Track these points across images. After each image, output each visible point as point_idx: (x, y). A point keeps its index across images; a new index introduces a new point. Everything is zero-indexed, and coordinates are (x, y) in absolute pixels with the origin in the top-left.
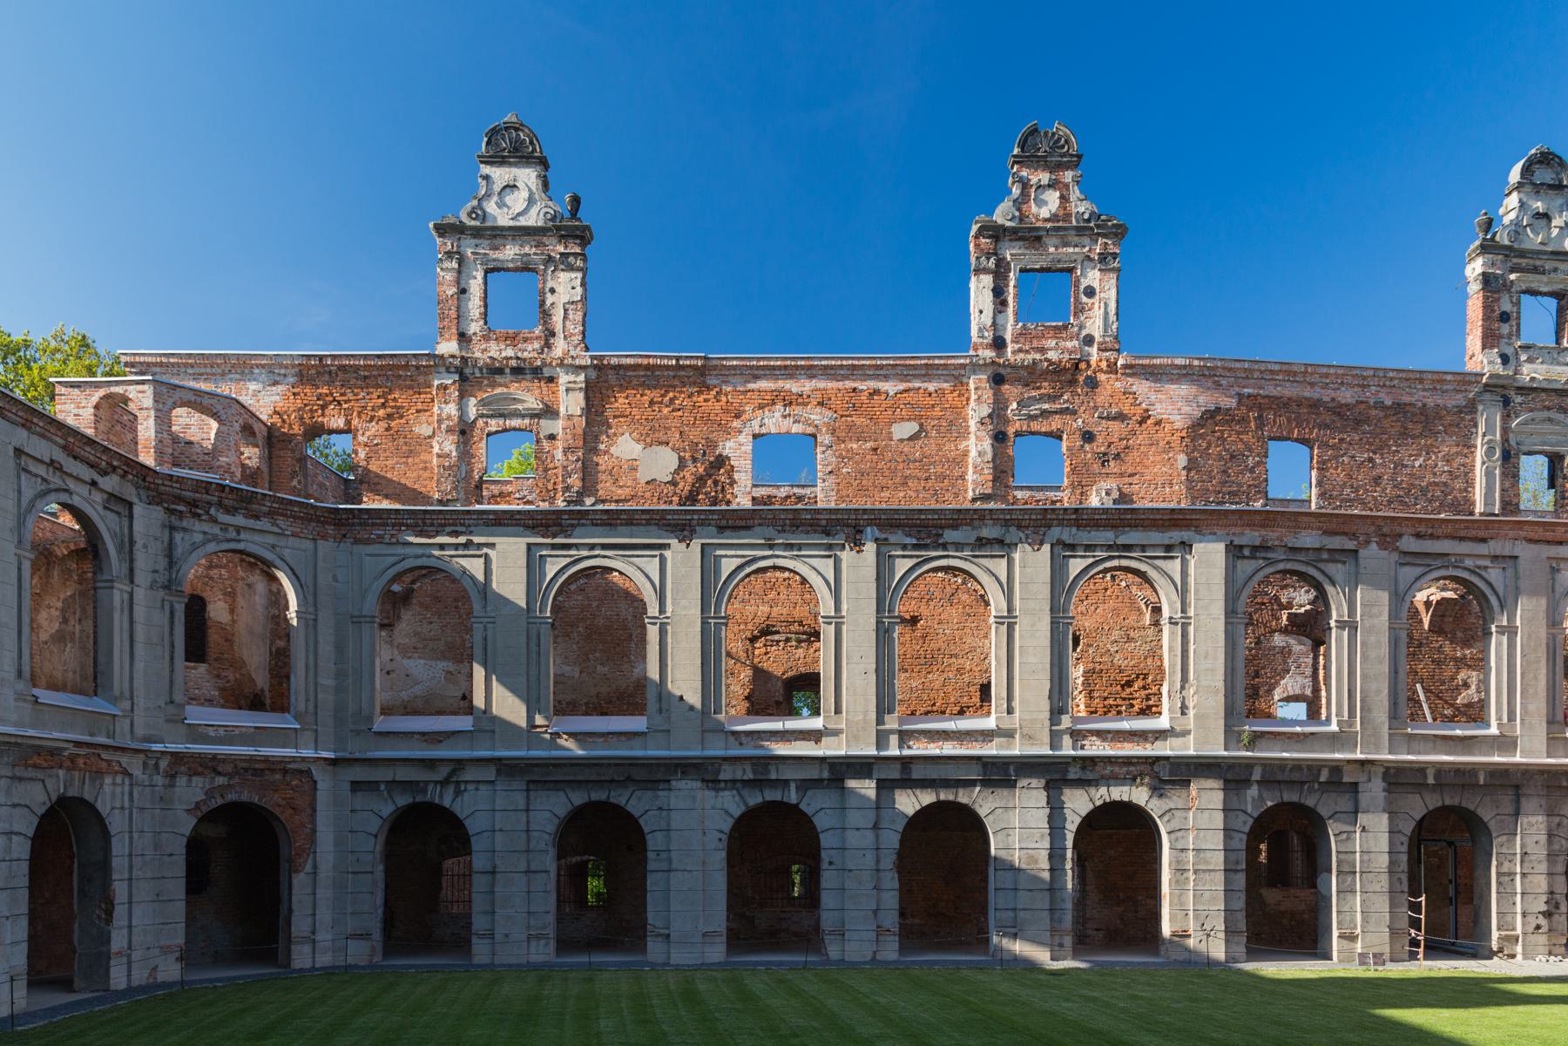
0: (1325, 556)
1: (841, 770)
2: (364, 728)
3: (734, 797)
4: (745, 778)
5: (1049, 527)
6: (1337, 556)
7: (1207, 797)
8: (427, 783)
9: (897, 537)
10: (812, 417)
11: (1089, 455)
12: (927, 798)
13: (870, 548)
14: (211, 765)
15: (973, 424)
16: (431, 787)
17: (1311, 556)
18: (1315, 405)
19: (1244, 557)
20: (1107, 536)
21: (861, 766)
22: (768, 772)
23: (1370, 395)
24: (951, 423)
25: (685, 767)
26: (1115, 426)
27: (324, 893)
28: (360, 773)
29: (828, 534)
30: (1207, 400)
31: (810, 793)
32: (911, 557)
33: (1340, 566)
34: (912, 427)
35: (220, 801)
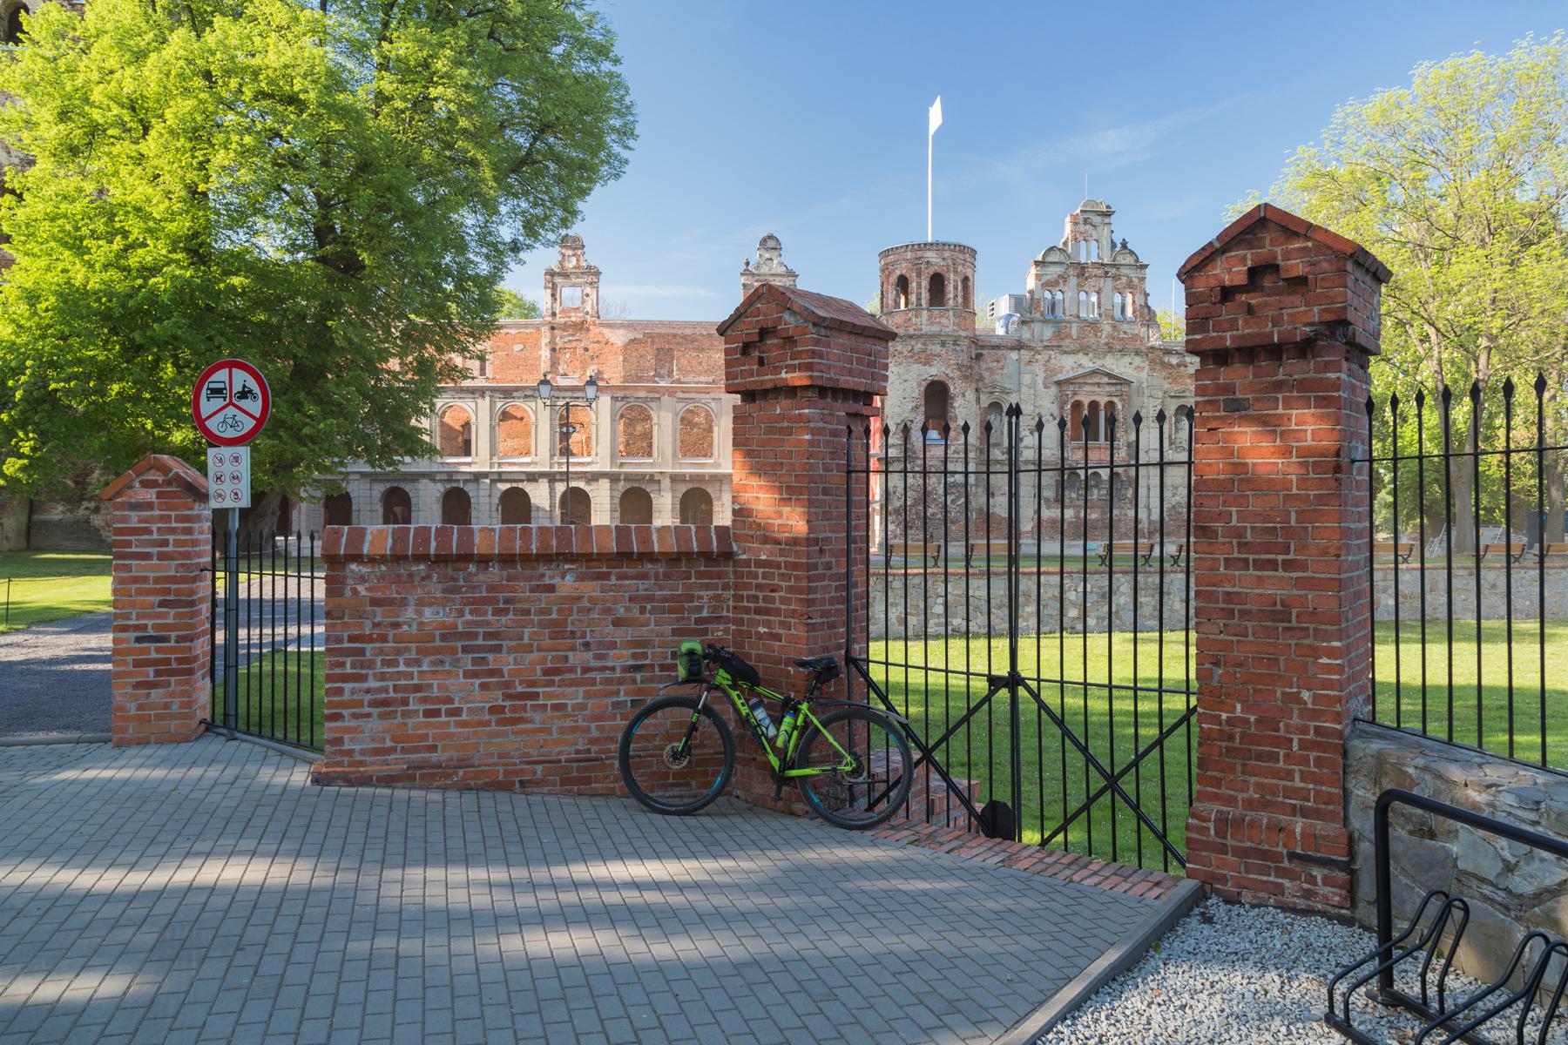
1: (478, 477)
7: (605, 484)
12: (508, 486)
13: (488, 399)
18: (675, 336)
20: (570, 394)
21: (485, 475)
23: (697, 331)
27: (303, 517)
30: (631, 336)
34: (521, 346)
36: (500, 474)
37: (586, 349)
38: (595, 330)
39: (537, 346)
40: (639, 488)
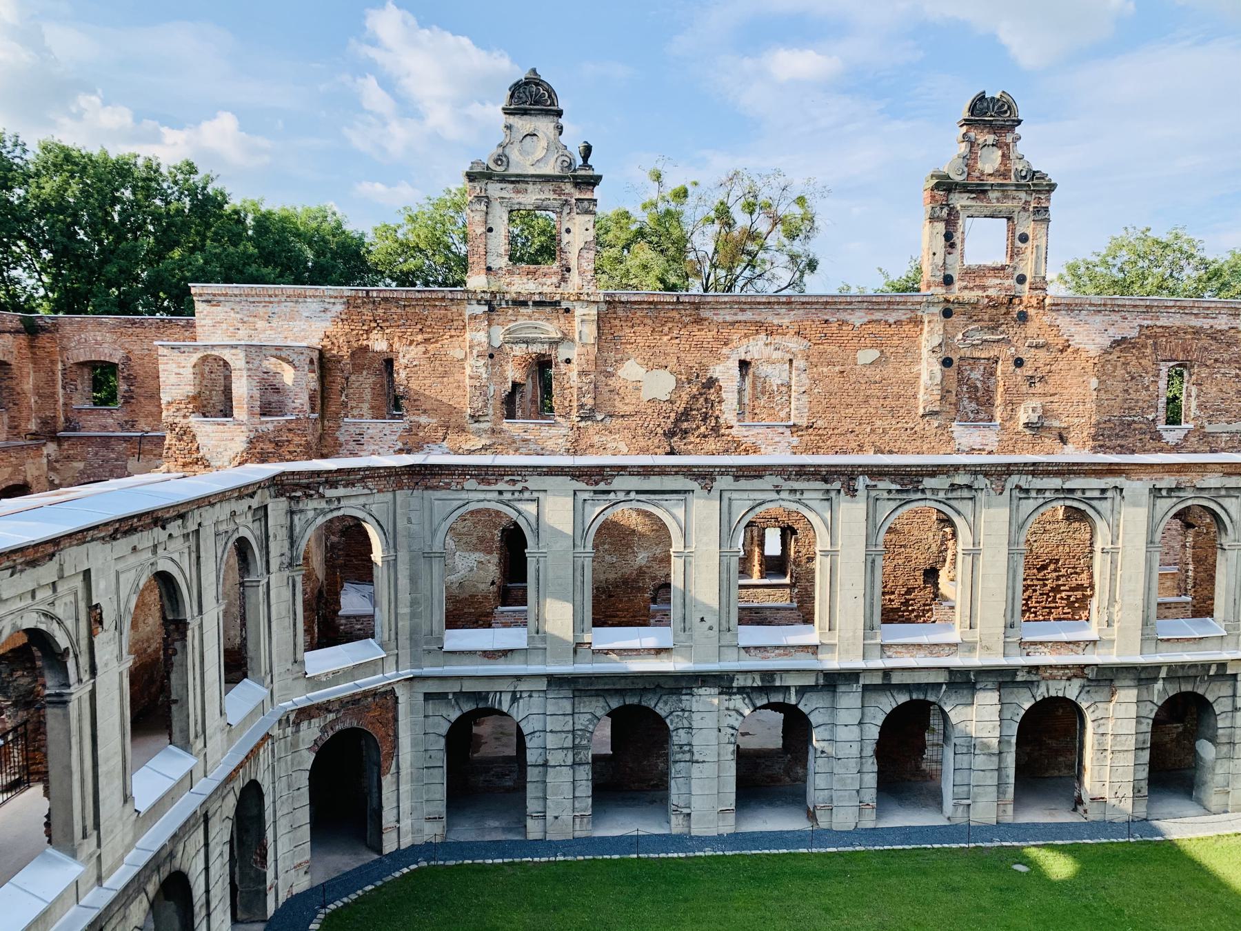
0: (1223, 492)
2: (435, 647)
3: (744, 699)
4: (755, 685)
5: (1010, 475)
6: (1232, 493)
8: (488, 693)
9: (885, 484)
10: (790, 345)
11: (1019, 378)
14: (324, 708)
15: (925, 352)
16: (491, 696)
17: (1213, 493)
19: (1163, 497)
20: (1056, 482)
22: (774, 680)
24: (907, 351)
25: (703, 679)
26: (1042, 354)
28: (433, 688)
29: (826, 481)
31: (807, 696)
32: (895, 499)
33: (1234, 500)
34: (875, 354)
35: (331, 733)
36: (887, 672)
37: (1019, 363)
38: (1039, 320)
39: (910, 354)
40: (1193, 694)
